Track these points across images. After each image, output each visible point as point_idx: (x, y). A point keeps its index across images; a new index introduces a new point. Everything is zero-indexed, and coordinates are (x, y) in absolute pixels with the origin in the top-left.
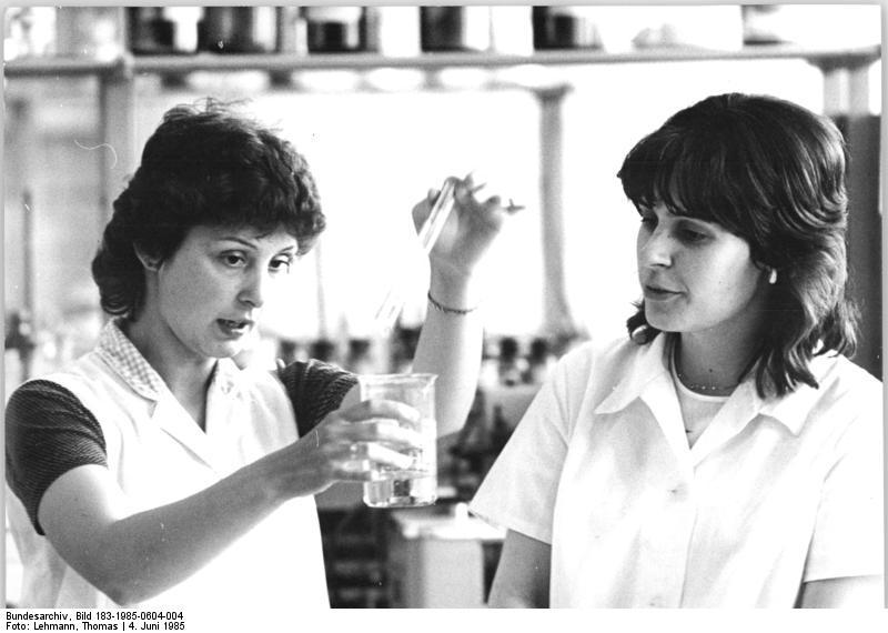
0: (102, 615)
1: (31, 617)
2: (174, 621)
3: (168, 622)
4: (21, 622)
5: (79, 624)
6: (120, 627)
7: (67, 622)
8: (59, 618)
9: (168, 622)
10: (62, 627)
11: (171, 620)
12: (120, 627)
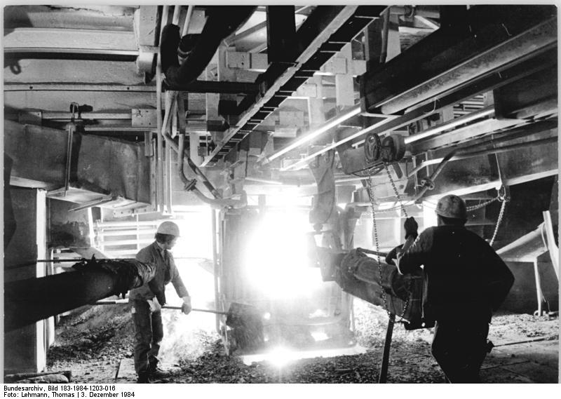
1: (20, 389)
4: (13, 392)
5: (50, 393)
6: (76, 395)
7: (42, 392)
8: (38, 389)
10: (39, 395)
12: (76, 395)
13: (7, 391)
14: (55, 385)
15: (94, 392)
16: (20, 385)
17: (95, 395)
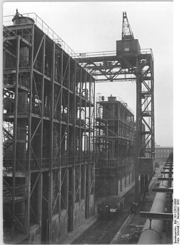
0: (175, 217)
1: (175, 236)
2: (177, 203)
3: (177, 204)
4: (177, 239)
8: (176, 229)
9: (177, 204)
11: (176, 203)
13: (177, 242)
14: (174, 221)
15: (177, 217)
16: (174, 236)
17: (178, 217)
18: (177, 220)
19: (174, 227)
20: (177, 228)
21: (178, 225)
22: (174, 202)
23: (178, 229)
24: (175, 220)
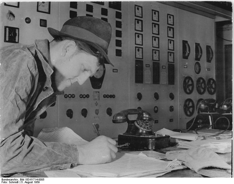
1: (8, 180)
4: (6, 181)
8: (16, 180)
13: (3, 181)
15: (27, 181)
18: (24, 182)
19: (17, 178)
20: (17, 181)
21: (19, 182)
22: (41, 178)
23: (16, 182)
24: (24, 180)
